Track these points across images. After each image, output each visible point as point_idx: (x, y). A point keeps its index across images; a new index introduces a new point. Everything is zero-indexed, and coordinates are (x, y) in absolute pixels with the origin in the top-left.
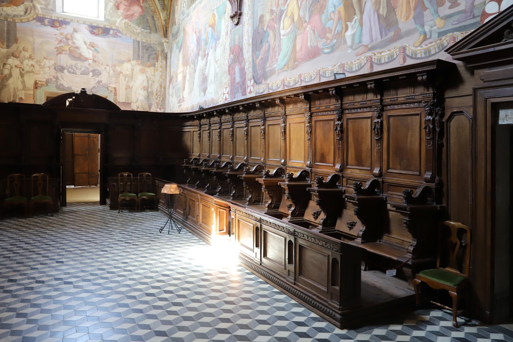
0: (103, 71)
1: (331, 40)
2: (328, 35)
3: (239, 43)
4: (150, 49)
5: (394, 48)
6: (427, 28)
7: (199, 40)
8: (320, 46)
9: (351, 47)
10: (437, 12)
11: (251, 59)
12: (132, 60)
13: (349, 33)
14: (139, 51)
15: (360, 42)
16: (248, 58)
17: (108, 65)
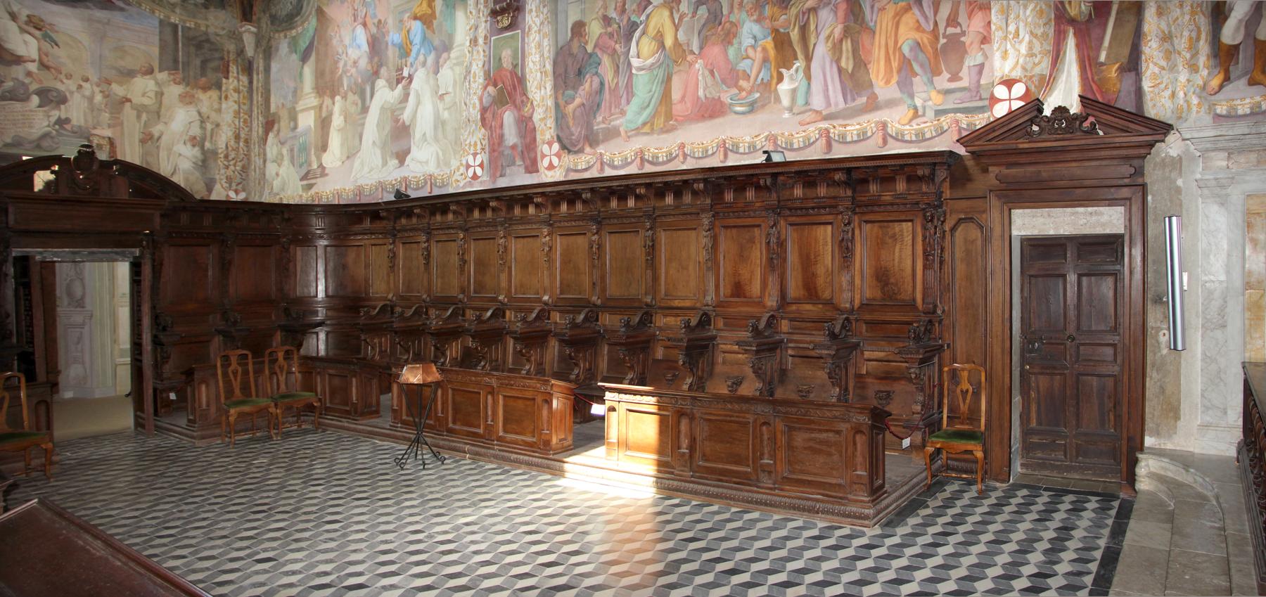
0: (72, 93)
1: (750, 93)
2: (742, 83)
3: (515, 66)
4: (207, 45)
5: (869, 122)
6: (918, 102)
7: (375, 45)
8: (726, 98)
9: (790, 109)
10: (932, 82)
11: (550, 103)
12: (156, 70)
13: (784, 87)
14: (177, 50)
15: (807, 103)
16: (543, 99)
17: (87, 80)
